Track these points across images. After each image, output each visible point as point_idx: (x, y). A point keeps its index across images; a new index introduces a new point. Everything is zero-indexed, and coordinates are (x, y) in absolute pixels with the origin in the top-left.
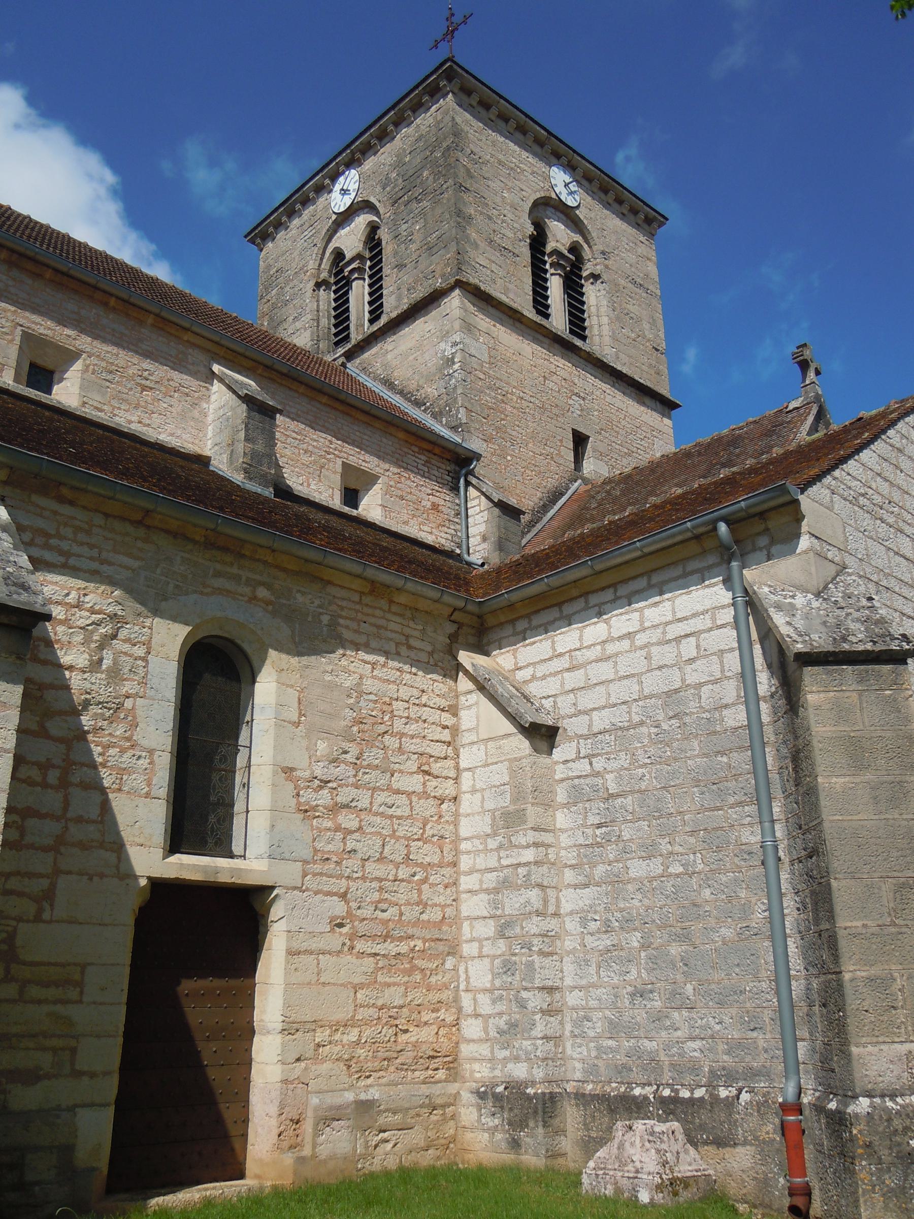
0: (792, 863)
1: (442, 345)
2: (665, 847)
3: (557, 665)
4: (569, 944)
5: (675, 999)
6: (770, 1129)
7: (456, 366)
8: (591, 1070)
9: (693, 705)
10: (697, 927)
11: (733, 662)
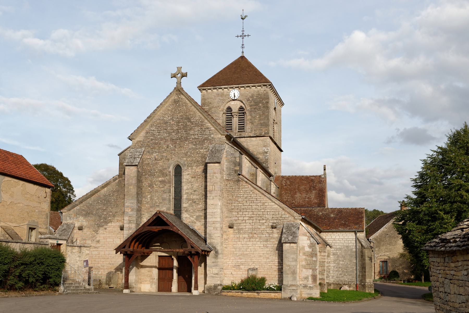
0: (359, 264)
1: (264, 148)
2: (345, 261)
3: (332, 239)
4: (332, 269)
5: (345, 275)
6: (355, 286)
7: (268, 154)
8: (334, 281)
9: (349, 248)
10: (348, 269)
11: (355, 245)
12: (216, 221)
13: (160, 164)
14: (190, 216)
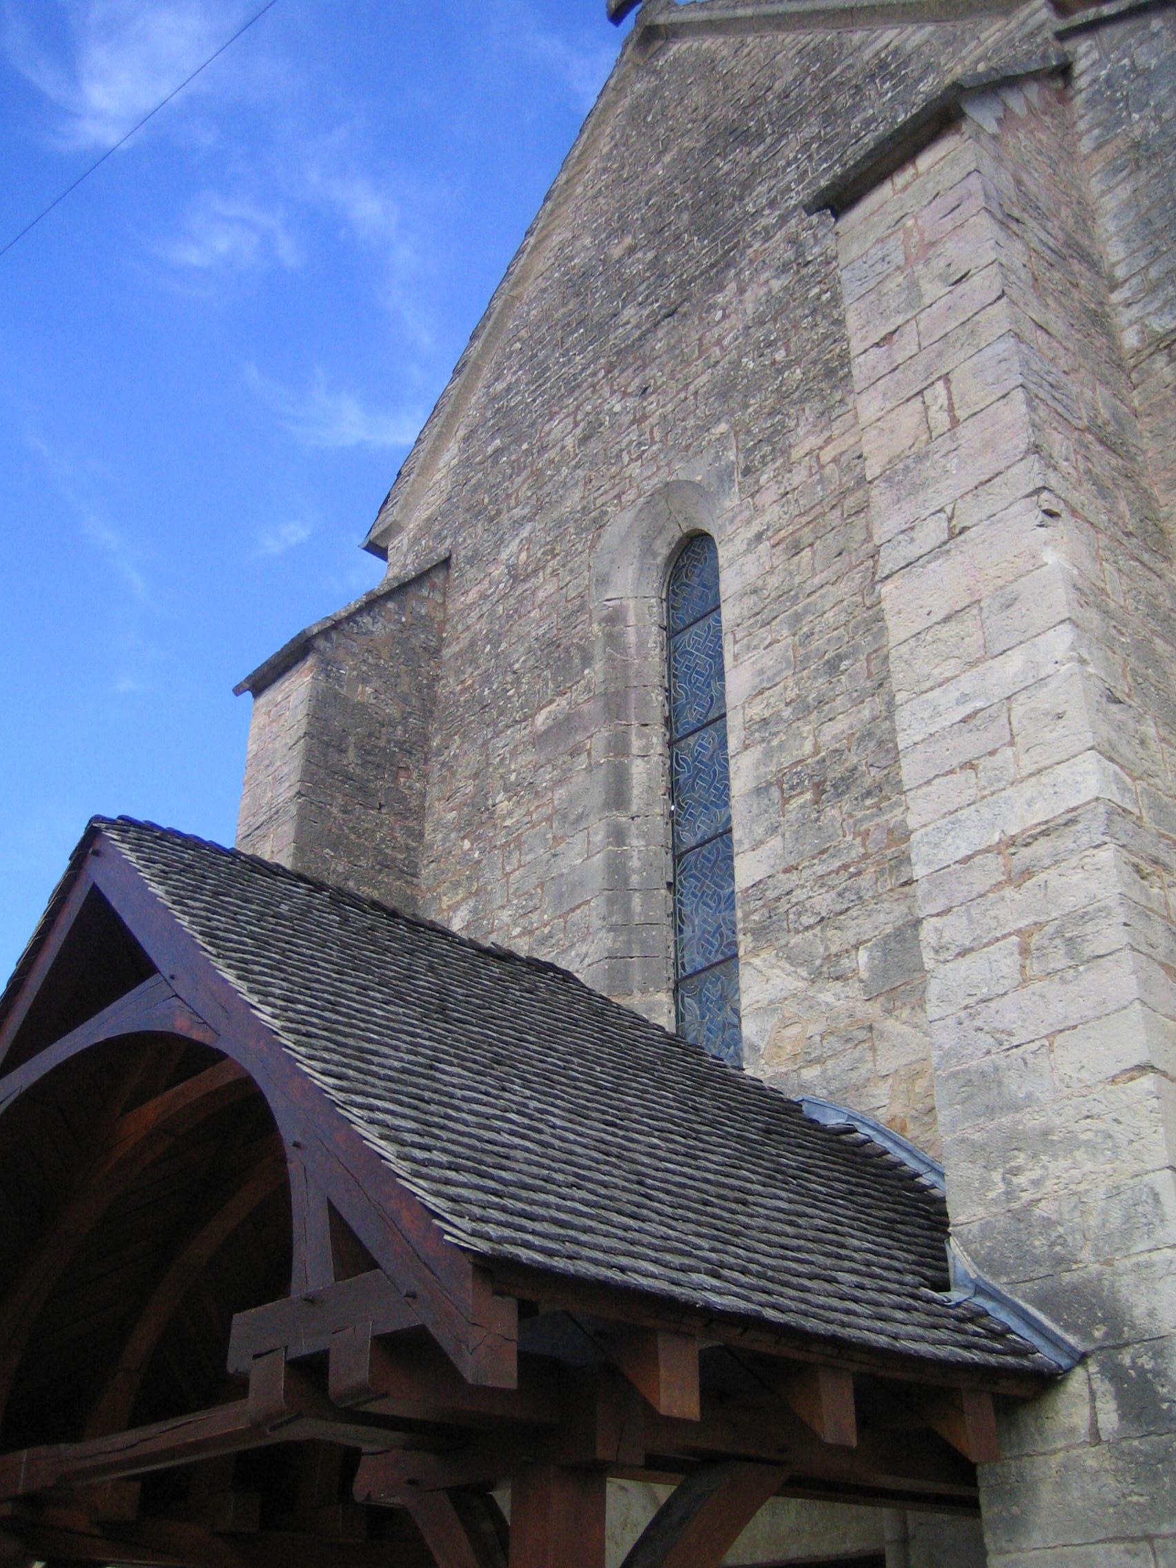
12: (1047, 829)
13: (541, 595)
14: (816, 976)
